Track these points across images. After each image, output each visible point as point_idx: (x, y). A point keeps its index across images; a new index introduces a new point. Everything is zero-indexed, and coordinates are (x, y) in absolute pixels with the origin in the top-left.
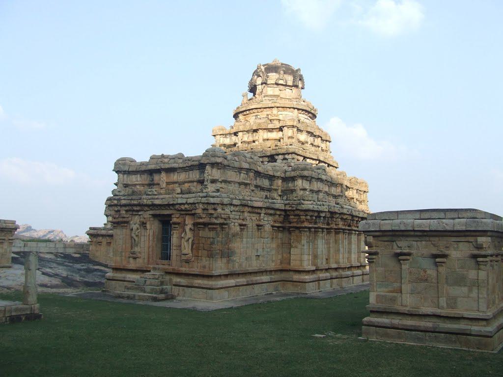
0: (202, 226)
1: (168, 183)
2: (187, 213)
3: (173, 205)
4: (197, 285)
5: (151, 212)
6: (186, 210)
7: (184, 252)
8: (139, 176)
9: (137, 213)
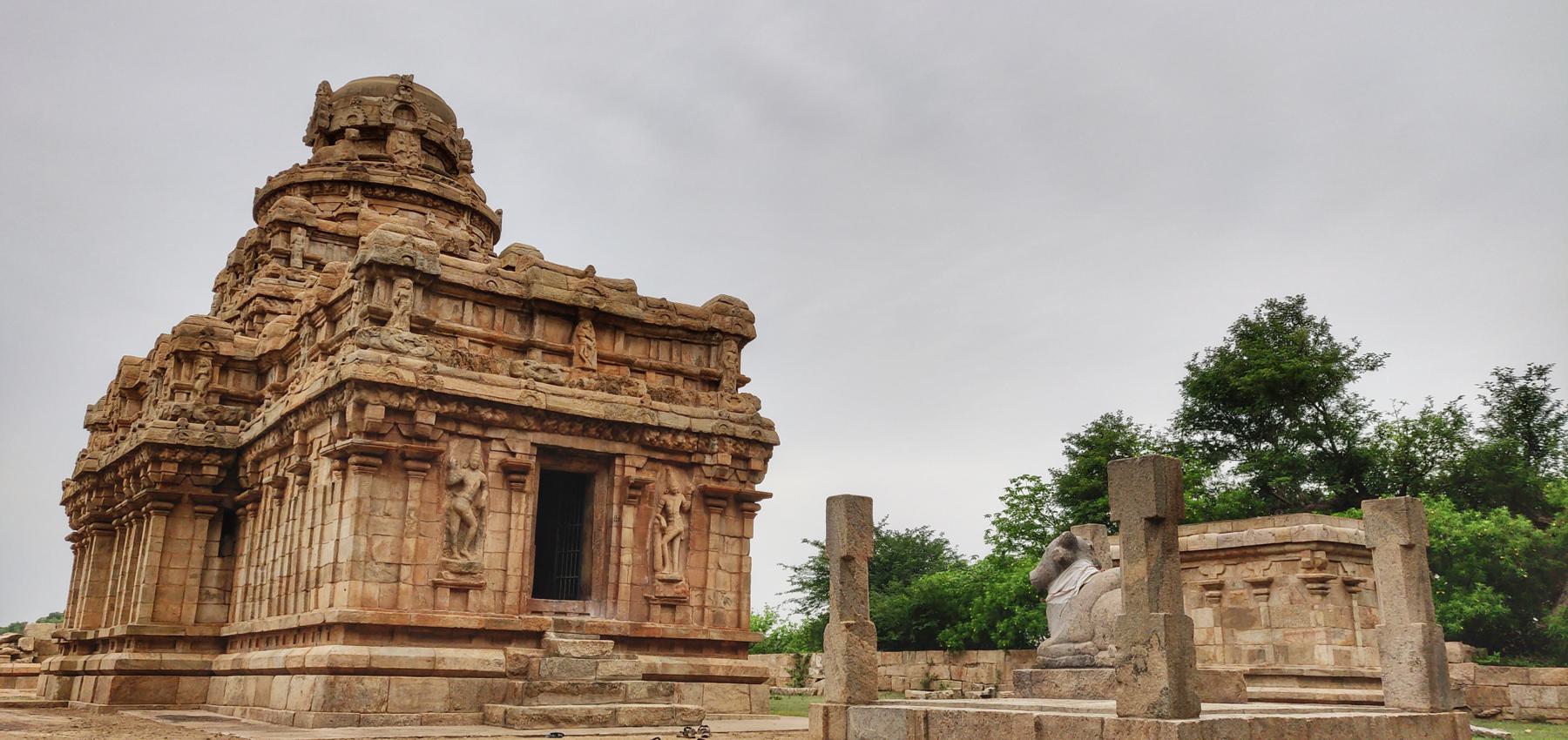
1: (602, 360)
3: (646, 427)
4: (720, 673)
6: (678, 450)
7: (667, 573)
8: (469, 306)
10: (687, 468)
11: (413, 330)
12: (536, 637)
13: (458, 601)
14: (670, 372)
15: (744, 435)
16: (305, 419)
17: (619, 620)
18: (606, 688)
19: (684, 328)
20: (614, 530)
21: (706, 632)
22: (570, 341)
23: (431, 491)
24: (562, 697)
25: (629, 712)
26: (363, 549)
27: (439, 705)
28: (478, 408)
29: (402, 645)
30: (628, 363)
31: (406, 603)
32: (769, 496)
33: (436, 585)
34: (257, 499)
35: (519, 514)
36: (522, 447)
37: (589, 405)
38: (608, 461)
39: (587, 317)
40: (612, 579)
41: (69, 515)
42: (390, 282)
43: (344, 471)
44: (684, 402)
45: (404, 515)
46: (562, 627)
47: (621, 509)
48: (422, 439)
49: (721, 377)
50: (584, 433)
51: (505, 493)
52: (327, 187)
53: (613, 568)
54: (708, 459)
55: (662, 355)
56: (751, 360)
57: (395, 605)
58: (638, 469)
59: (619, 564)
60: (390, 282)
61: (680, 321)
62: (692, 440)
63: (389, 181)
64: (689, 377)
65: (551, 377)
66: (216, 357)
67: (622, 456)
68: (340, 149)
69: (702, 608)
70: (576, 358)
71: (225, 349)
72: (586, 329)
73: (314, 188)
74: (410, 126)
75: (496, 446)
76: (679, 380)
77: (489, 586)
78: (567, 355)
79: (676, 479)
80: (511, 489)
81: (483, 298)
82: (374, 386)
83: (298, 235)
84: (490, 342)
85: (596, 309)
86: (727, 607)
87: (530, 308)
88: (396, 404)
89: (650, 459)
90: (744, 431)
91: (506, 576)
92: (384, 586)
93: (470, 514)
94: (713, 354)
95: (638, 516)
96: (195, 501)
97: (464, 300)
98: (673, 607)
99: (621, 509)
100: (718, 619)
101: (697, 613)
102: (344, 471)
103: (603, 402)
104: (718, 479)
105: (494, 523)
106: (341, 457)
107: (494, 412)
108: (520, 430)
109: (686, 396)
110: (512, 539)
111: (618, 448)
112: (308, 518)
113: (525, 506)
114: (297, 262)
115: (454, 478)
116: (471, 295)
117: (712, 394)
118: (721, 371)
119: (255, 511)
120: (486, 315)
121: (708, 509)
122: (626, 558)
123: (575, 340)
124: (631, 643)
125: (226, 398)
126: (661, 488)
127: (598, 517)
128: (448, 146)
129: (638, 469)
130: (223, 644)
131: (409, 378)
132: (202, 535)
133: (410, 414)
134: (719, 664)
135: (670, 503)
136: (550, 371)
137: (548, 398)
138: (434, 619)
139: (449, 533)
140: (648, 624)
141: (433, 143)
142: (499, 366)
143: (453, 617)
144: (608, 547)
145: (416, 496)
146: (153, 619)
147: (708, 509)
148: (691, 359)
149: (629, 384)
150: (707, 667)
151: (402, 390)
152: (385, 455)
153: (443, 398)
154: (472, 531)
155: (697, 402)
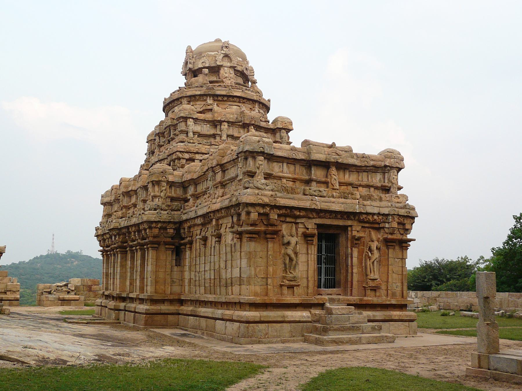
0: (156, 246)
1: (341, 184)
2: (372, 226)
3: (361, 213)
4: (397, 318)
5: (319, 221)
6: (374, 222)
7: (372, 276)
8: (285, 164)
9: (293, 220)
10: (378, 229)
11: (265, 178)
12: (321, 306)
13: (290, 291)
14: (368, 186)
15: (403, 214)
16: (218, 215)
17: (355, 298)
18: (354, 329)
19: (373, 166)
20: (349, 259)
21: (390, 301)
22: (327, 177)
23: (277, 246)
24: (338, 332)
25: (365, 337)
26: (253, 273)
27: (287, 335)
28: (293, 210)
29: (271, 311)
30: (351, 184)
31: (271, 294)
32: (414, 240)
33: (281, 286)
34: (191, 243)
35: (311, 254)
36: (311, 225)
37: (337, 205)
38: (345, 228)
39: (333, 165)
40: (349, 279)
41: (100, 241)
42: (254, 158)
43: (241, 239)
44: (375, 200)
45: (267, 257)
46: (332, 301)
47: (352, 249)
48: (272, 225)
49: (390, 187)
50: (336, 218)
51: (305, 246)
52: (197, 97)
53: (349, 275)
54: (387, 225)
55: (364, 178)
56: (402, 178)
57: (267, 295)
58: (358, 231)
59: (352, 273)
60: (254, 158)
61: (372, 163)
62: (380, 217)
63: (224, 93)
64: (376, 188)
65: (320, 193)
66: (168, 182)
67: (351, 226)
68: (200, 79)
69: (387, 290)
70: (330, 184)
71: (171, 179)
72: (333, 171)
73: (192, 98)
74: (229, 64)
75: (301, 226)
76: (372, 189)
77: (302, 285)
78: (326, 183)
79: (374, 234)
80: (307, 243)
81: (290, 161)
82: (253, 205)
83: (190, 122)
84: (294, 180)
85: (337, 162)
86: (398, 289)
87: (309, 164)
88: (262, 212)
89: (362, 227)
90: (402, 212)
91: (308, 281)
92: (262, 287)
93: (293, 256)
94: (386, 176)
95: (359, 252)
96: (166, 243)
97: (283, 162)
98: (375, 290)
99: (352, 249)
100: (394, 295)
101: (385, 292)
102: (241, 239)
103: (343, 203)
104: (391, 234)
105: (302, 258)
106: (240, 234)
107: (300, 212)
108: (310, 218)
109: (376, 197)
110: (310, 265)
111: (349, 223)
112: (223, 257)
113: (313, 250)
114: (191, 134)
115: (286, 241)
116: (286, 160)
117: (387, 195)
118: (390, 185)
119: (191, 248)
120: (292, 167)
121: (388, 247)
122: (355, 271)
123: (329, 177)
124: (360, 306)
125: (173, 199)
126: (368, 239)
127: (342, 253)
128: (245, 71)
129: (358, 231)
130: (181, 302)
131: (266, 200)
132: (169, 258)
133: (266, 215)
134: (396, 314)
135: (372, 246)
136: (320, 191)
137: (320, 204)
138: (282, 300)
139: (285, 264)
140: (365, 298)
141: (238, 71)
142: (299, 190)
143: (289, 299)
144: (347, 266)
145: (272, 249)
146: (156, 292)
147: (388, 247)
148: (377, 179)
149: (352, 194)
150: (391, 316)
151: (263, 206)
152: (257, 233)
153: (280, 207)
154: (294, 262)
155: (381, 199)
